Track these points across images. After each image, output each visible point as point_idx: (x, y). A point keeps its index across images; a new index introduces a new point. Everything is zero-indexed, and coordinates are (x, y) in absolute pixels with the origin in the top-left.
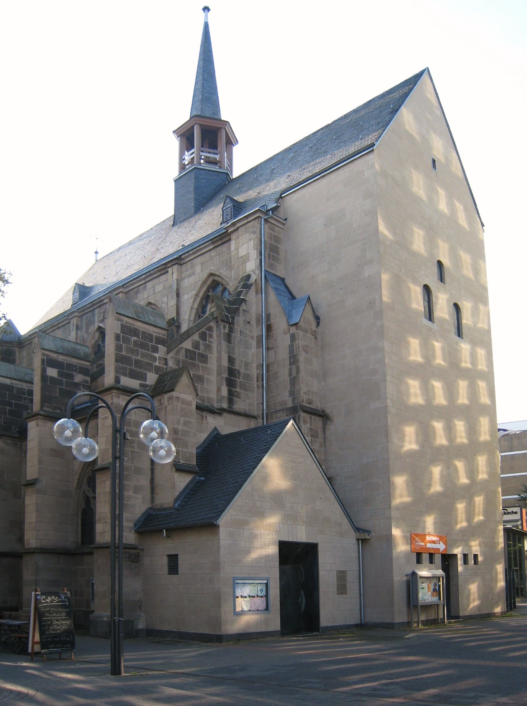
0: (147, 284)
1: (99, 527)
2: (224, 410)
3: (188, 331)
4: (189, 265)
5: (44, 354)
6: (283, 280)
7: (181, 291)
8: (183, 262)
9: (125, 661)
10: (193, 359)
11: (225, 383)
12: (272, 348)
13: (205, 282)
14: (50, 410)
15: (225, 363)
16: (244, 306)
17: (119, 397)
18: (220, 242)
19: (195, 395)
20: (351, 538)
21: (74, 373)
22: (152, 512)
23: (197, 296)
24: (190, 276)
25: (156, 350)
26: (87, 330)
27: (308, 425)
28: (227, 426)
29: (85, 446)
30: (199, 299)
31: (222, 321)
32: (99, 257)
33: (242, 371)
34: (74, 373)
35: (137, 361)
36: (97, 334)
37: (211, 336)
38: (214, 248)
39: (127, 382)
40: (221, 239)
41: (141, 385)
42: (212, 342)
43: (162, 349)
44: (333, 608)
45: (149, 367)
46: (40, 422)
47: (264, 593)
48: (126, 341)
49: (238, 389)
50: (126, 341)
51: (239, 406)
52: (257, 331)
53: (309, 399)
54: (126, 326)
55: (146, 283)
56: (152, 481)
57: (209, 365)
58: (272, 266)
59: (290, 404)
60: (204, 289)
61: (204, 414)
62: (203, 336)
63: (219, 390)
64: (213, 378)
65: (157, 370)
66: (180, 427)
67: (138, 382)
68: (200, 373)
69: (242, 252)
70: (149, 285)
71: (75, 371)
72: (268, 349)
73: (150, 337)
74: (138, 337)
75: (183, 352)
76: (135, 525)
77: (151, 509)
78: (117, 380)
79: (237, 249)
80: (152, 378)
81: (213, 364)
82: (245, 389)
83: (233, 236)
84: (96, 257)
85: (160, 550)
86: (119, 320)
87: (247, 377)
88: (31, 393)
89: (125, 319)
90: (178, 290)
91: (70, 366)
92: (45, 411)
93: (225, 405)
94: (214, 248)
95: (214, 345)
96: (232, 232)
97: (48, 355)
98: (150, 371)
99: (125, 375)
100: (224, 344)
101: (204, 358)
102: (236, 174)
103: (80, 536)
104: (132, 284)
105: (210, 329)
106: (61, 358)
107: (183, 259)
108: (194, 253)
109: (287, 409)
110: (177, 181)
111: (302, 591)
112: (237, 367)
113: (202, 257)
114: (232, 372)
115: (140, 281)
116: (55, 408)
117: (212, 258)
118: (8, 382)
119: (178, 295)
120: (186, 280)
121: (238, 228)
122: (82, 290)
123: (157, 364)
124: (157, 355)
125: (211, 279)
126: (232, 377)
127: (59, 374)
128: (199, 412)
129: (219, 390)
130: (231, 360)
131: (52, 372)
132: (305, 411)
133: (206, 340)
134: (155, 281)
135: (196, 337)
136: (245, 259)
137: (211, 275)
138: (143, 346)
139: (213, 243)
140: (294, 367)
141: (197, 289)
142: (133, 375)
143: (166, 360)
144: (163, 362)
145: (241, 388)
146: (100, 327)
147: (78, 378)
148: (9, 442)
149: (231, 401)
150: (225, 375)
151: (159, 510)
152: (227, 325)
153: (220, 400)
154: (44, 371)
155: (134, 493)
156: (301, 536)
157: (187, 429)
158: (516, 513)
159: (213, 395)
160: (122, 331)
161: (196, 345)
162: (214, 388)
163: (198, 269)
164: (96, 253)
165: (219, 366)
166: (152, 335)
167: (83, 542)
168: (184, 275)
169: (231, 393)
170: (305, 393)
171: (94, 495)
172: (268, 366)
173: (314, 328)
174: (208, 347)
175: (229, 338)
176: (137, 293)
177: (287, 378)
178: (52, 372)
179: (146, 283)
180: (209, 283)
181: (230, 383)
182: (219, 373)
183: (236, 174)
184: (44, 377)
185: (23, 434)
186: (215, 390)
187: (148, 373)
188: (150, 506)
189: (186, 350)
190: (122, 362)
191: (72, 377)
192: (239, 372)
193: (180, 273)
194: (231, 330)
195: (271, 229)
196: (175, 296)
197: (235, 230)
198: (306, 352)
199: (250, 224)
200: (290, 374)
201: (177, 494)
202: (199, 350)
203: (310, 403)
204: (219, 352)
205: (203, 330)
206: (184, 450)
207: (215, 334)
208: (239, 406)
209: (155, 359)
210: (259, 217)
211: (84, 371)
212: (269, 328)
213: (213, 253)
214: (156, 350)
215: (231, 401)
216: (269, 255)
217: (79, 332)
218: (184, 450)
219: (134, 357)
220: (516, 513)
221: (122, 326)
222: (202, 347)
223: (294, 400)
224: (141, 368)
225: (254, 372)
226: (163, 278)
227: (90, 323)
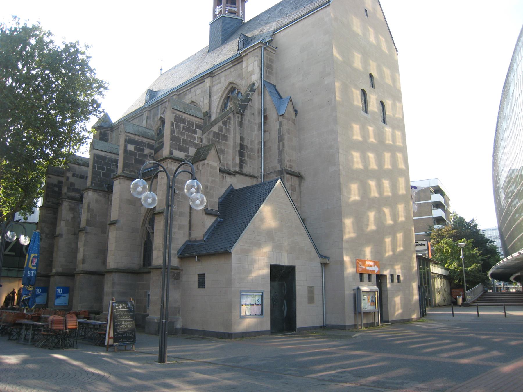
1: (155, 254)
2: (237, 172)
3: (215, 120)
4: (217, 77)
5: (126, 136)
6: (275, 86)
7: (212, 94)
8: (213, 75)
9: (169, 352)
10: (218, 138)
11: (237, 154)
12: (267, 131)
13: (227, 88)
14: (128, 173)
15: (238, 141)
16: (250, 104)
17: (171, 164)
18: (237, 63)
19: (219, 162)
20: (317, 262)
21: (145, 148)
22: (189, 243)
23: (222, 97)
24: (218, 84)
26: (153, 119)
27: (290, 183)
28: (239, 183)
29: (149, 198)
30: (223, 99)
31: (237, 113)
32: (163, 72)
33: (249, 146)
34: (145, 148)
36: (159, 122)
37: (230, 123)
38: (233, 66)
39: (177, 154)
40: (237, 60)
41: (186, 156)
43: (199, 131)
44: (306, 314)
46: (122, 181)
47: (260, 302)
49: (246, 158)
51: (247, 169)
52: (258, 119)
53: (290, 165)
54: (178, 117)
56: (190, 221)
57: (228, 142)
58: (268, 77)
59: (278, 169)
60: (227, 92)
61: (224, 175)
62: (225, 123)
63: (234, 159)
64: (231, 151)
65: (196, 145)
66: (209, 184)
69: (250, 69)
70: (193, 90)
71: (145, 146)
72: (265, 131)
74: (185, 124)
76: (178, 253)
77: (188, 241)
78: (171, 153)
79: (247, 67)
80: (192, 151)
81: (230, 142)
82: (250, 158)
83: (245, 59)
85: (193, 269)
86: (174, 113)
87: (252, 150)
88: (117, 161)
89: (177, 112)
90: (210, 93)
91: (142, 143)
92: (124, 173)
93: (237, 169)
94: (233, 66)
95: (232, 129)
96: (244, 56)
100: (238, 128)
101: (225, 138)
102: (247, 20)
103: (142, 261)
104: (182, 90)
105: (229, 118)
106: (137, 138)
107: (214, 73)
108: (221, 69)
109: (277, 172)
110: (211, 24)
111: (285, 301)
112: (245, 143)
113: (226, 72)
114: (242, 147)
115: (187, 87)
116: (131, 171)
117: (231, 72)
118: (103, 154)
119: (210, 96)
120: (215, 87)
121: (247, 54)
122: (151, 94)
123: (196, 142)
125: (231, 86)
126: (242, 150)
127: (136, 148)
128: (221, 174)
129: (234, 159)
130: (242, 139)
131: (131, 147)
132: (287, 173)
133: (226, 126)
134: (196, 87)
135: (220, 124)
136: (252, 73)
137: (231, 83)
139: (232, 63)
140: (281, 143)
141: (222, 92)
143: (202, 139)
145: (247, 158)
146: (161, 118)
147: (147, 151)
148: (101, 194)
149: (241, 167)
151: (193, 242)
152: (240, 116)
153: (234, 166)
154: (126, 146)
155: (179, 229)
156: (285, 261)
157: (213, 186)
158: (424, 245)
159: (230, 163)
160: (175, 120)
161: (221, 129)
162: (231, 158)
163: (223, 79)
164: (161, 69)
165: (235, 143)
166: (193, 123)
167: (144, 265)
168: (214, 83)
169: (241, 161)
170: (288, 161)
171: (152, 231)
172: (265, 143)
173: (294, 118)
174: (228, 130)
175: (241, 124)
176: (185, 95)
177: (277, 151)
178: (131, 147)
180: (229, 88)
182: (234, 148)
183: (247, 20)
184: (126, 151)
185: (110, 189)
186: (231, 159)
187: (190, 148)
188: (188, 239)
190: (174, 141)
191: (142, 150)
192: (247, 147)
193: (212, 82)
194: (242, 119)
195: (267, 54)
196: (208, 97)
197: (246, 55)
198: (289, 133)
199: (256, 50)
200: (279, 149)
201: (206, 230)
202: (222, 132)
203: (291, 168)
204: (235, 133)
205: (225, 119)
206: (211, 200)
207: (232, 122)
209: (195, 138)
211: (151, 147)
212: (266, 117)
213: (232, 69)
215: (241, 167)
216: (266, 70)
217: (148, 121)
218: (211, 200)
220: (424, 245)
221: (176, 117)
222: (224, 130)
223: (281, 165)
224: (186, 144)
225: (256, 147)
226: (201, 85)
227: (155, 115)
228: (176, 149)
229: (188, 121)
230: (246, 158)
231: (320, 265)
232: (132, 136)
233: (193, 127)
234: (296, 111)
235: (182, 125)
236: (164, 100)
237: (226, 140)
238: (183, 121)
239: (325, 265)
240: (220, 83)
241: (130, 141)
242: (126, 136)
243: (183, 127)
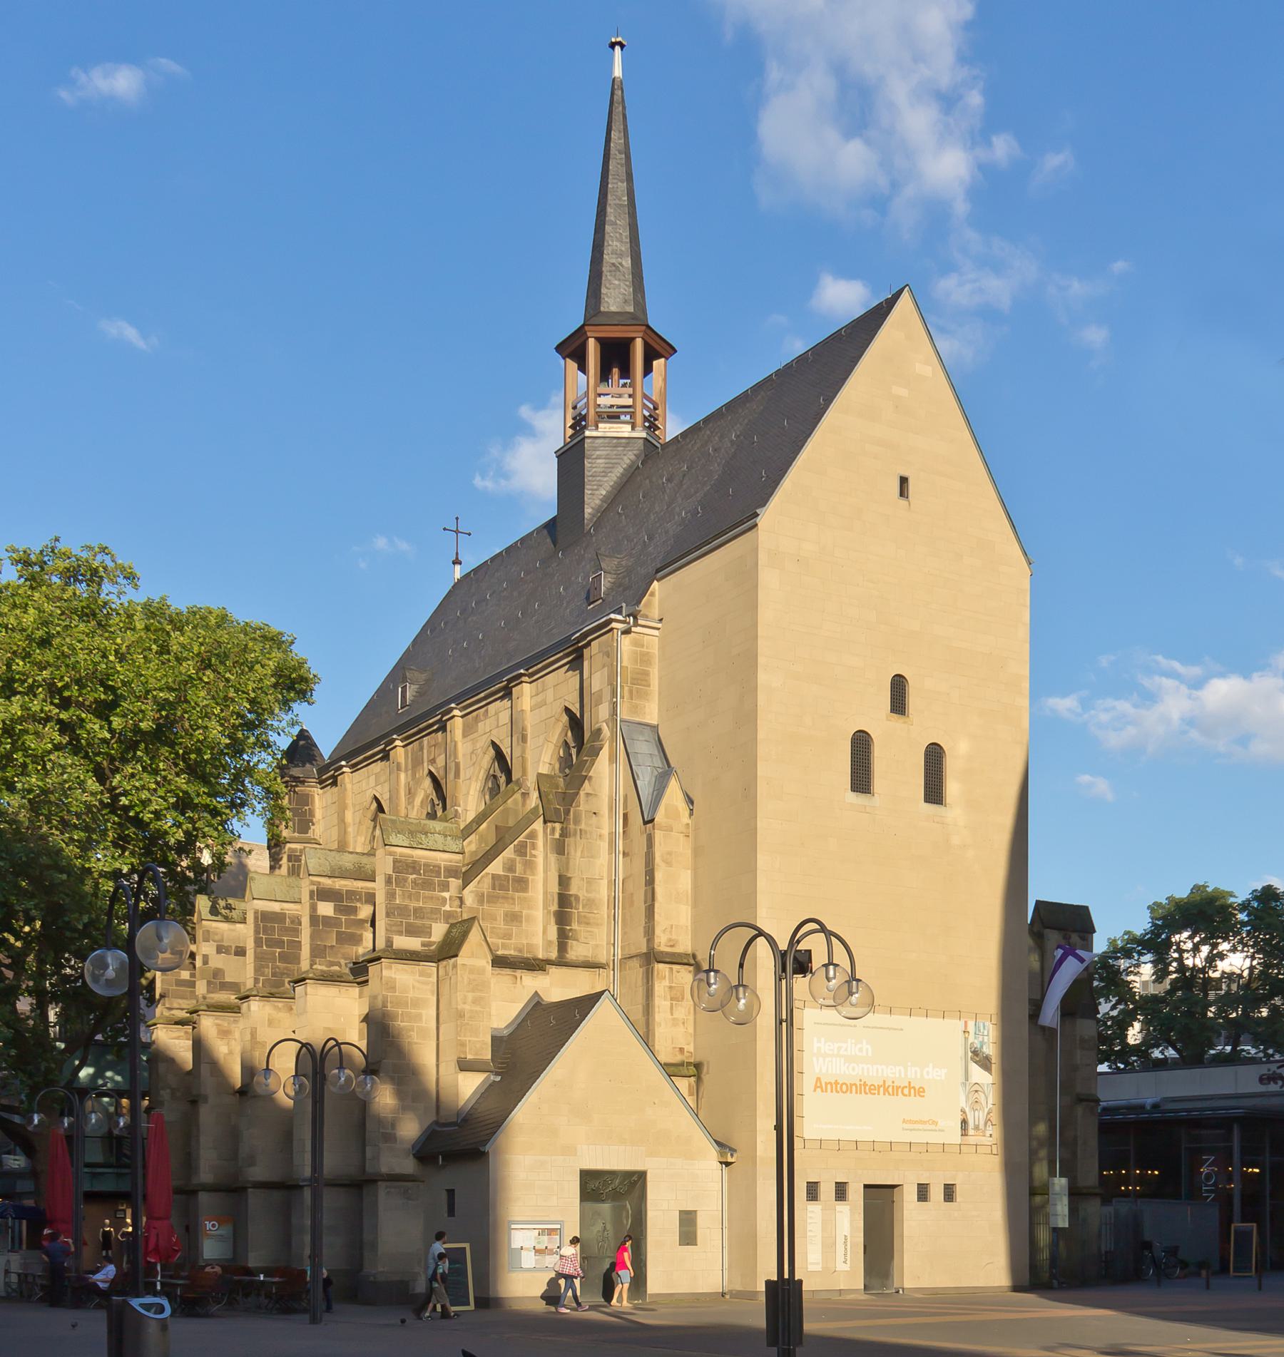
11: (553, 920)
15: (555, 889)
25: (445, 887)
28: (558, 987)
35: (416, 910)
39: (404, 942)
62: (521, 850)
67: (420, 940)
75: (488, 881)
87: (590, 903)
93: (554, 955)
98: (436, 920)
99: (400, 933)
100: (553, 858)
101: (522, 884)
124: (446, 895)
130: (564, 881)
142: (411, 931)
144: (457, 902)
149: (562, 947)
150: (555, 907)
159: (538, 941)
161: (510, 867)
165: (545, 893)
174: (530, 865)
181: (562, 918)
186: (538, 934)
189: (494, 877)
204: (545, 871)
208: (577, 951)
214: (445, 887)
215: (562, 947)
219: (413, 904)
222: (519, 867)
230: (575, 926)
237: (525, 889)
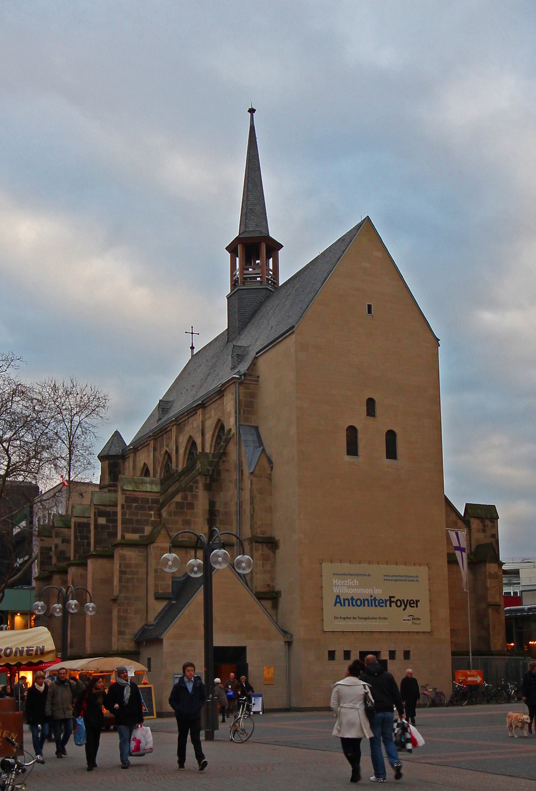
0: (190, 419)
35: (137, 520)
37: (197, 487)
42: (198, 492)
45: (146, 522)
48: (129, 507)
50: (129, 507)
52: (235, 476)
55: (188, 418)
57: (195, 510)
68: (188, 518)
73: (147, 501)
84: (192, 352)
97: (98, 508)
98: (146, 525)
101: (191, 506)
104: (181, 419)
105: (196, 482)
110: (229, 298)
126: (212, 516)
127: (107, 521)
131: (102, 521)
133: (192, 491)
138: (142, 508)
141: (212, 431)
142: (134, 531)
150: (207, 517)
154: (96, 520)
174: (195, 497)
176: (185, 425)
177: (249, 514)
178: (102, 521)
179: (188, 418)
184: (96, 526)
189: (177, 503)
192: (219, 511)
193: (204, 414)
203: (263, 534)
205: (191, 484)
210: (234, 382)
216: (244, 411)
219: (135, 518)
222: (189, 498)
228: (128, 532)
229: (142, 499)
231: (282, 643)
232: (102, 508)
233: (148, 503)
234: (270, 462)
235: (135, 504)
236: (166, 428)
238: (136, 500)
239: (289, 644)
240: (210, 417)
241: (99, 514)
242: (95, 509)
243: (136, 507)
